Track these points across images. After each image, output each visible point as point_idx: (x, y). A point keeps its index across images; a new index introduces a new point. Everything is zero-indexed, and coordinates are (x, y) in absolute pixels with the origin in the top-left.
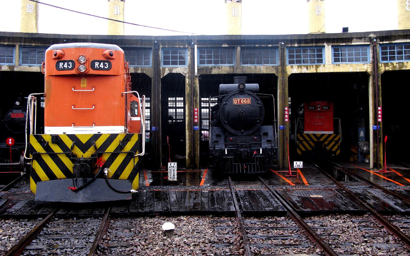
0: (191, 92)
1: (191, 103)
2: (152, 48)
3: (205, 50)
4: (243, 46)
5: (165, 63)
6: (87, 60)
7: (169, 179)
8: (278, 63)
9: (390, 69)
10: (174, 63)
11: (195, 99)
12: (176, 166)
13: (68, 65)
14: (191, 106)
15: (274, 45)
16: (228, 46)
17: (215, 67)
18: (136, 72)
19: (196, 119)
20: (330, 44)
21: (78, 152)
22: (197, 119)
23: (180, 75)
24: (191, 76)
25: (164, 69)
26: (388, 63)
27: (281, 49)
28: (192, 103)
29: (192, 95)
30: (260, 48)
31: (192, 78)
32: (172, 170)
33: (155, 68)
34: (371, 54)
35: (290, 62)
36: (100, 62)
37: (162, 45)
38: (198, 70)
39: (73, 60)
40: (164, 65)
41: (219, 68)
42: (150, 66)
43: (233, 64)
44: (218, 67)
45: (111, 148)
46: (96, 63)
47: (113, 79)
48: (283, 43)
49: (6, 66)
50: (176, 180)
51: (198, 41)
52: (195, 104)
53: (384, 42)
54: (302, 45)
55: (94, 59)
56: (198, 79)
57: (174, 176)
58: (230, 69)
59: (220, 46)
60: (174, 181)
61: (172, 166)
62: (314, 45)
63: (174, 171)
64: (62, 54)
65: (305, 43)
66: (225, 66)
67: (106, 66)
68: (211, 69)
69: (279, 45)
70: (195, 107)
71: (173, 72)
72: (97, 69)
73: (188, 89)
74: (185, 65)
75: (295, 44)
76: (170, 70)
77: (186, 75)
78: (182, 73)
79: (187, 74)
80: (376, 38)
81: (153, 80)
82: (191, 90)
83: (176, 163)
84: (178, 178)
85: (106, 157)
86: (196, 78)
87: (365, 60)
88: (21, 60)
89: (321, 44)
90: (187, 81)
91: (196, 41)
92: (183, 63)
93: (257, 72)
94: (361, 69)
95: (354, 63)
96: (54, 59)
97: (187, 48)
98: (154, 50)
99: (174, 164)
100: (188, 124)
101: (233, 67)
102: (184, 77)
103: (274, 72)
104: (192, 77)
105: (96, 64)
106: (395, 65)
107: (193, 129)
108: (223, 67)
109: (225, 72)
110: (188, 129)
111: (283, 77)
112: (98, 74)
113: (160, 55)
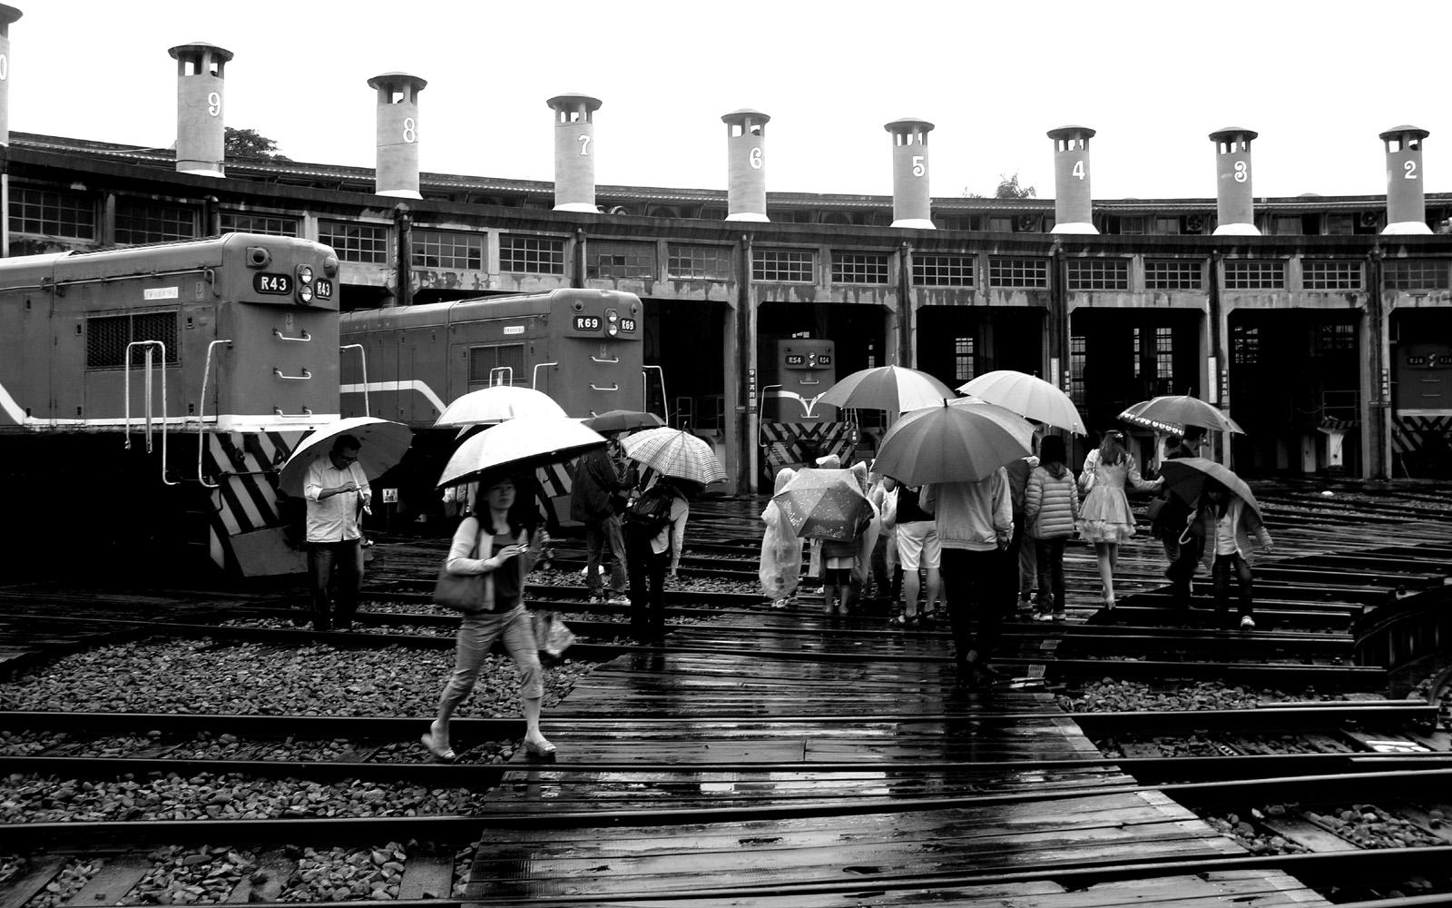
3: (21, 192)
9: (431, 286)
13: (279, 284)
20: (315, 213)
26: (427, 272)
34: (396, 248)
53: (422, 225)
54: (256, 209)
62: (282, 211)
72: (265, 292)
80: (409, 213)
87: (380, 259)
89: (296, 213)
94: (374, 281)
95: (363, 265)
106: (440, 277)
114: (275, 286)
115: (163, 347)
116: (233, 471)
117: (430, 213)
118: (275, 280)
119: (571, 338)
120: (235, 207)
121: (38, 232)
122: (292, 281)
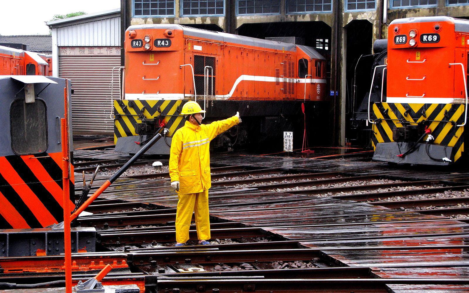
5: (351, 7)
6: (151, 40)
7: (285, 149)
10: (361, 6)
12: (292, 136)
13: (139, 43)
21: (147, 114)
23: (366, 21)
25: (347, 15)
32: (288, 140)
36: (162, 40)
39: (142, 39)
40: (348, 9)
44: (414, 10)
45: (171, 112)
46: (158, 41)
47: (173, 55)
49: (165, 19)
50: (291, 151)
55: (157, 38)
57: (289, 146)
60: (290, 152)
61: (287, 136)
63: (290, 140)
64: (134, 34)
67: (167, 44)
71: (357, 19)
76: (355, 16)
79: (375, 21)
83: (292, 133)
84: (294, 149)
85: (167, 120)
88: (182, 11)
96: (130, 38)
99: (290, 134)
105: (158, 42)
108: (420, 10)
112: (159, 50)
114: (163, 44)
115: (207, 66)
116: (124, 114)
118: (163, 42)
119: (393, 49)
122: (142, 42)
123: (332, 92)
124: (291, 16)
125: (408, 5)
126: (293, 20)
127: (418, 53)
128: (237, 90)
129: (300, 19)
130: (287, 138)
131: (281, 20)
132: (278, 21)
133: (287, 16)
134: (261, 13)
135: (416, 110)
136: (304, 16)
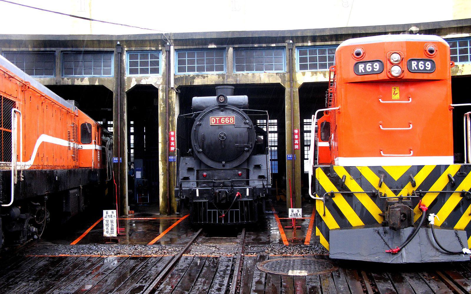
0: (166, 110)
1: (166, 125)
2: (114, 51)
4: (236, 46)
5: (132, 72)
8: (285, 69)
11: (170, 119)
12: (116, 216)
14: (165, 129)
15: (280, 45)
16: (216, 47)
17: (198, 76)
18: (92, 84)
19: (172, 146)
22: (174, 146)
24: (166, 88)
25: (130, 79)
27: (289, 49)
28: (167, 124)
29: (167, 114)
30: (260, 48)
31: (168, 90)
32: (110, 221)
33: (117, 79)
35: (303, 67)
37: (127, 47)
38: (176, 80)
41: (204, 77)
42: (112, 75)
43: (223, 70)
44: (202, 76)
48: (291, 42)
50: (115, 235)
51: (175, 40)
52: (171, 127)
54: (318, 43)
56: (175, 92)
57: (112, 229)
58: (219, 78)
59: (204, 47)
63: (112, 222)
65: (322, 41)
66: (212, 74)
68: (194, 78)
69: (286, 44)
70: (171, 130)
71: (141, 83)
73: (162, 106)
74: (159, 73)
75: (308, 42)
77: (159, 87)
78: (153, 84)
81: (114, 95)
82: (166, 107)
86: (172, 91)
90: (161, 95)
91: (172, 41)
92: (155, 71)
93: (256, 81)
97: (161, 50)
98: (116, 55)
99: (113, 212)
100: (162, 153)
101: (223, 75)
102: (157, 90)
103: (279, 81)
104: (167, 90)
107: (168, 161)
108: (209, 76)
109: (212, 82)
110: (161, 161)
111: (291, 87)
113: (125, 61)
117: (436, 29)
120: (305, 44)
121: (194, 71)
123: (115, 159)
124: (68, 79)
125: (195, 71)
126: (69, 83)
127: (395, 89)
128: (38, 155)
129: (78, 83)
130: (108, 218)
131: (57, 83)
132: (52, 84)
133: (63, 79)
134: (33, 75)
135: (396, 176)
136: (82, 80)
